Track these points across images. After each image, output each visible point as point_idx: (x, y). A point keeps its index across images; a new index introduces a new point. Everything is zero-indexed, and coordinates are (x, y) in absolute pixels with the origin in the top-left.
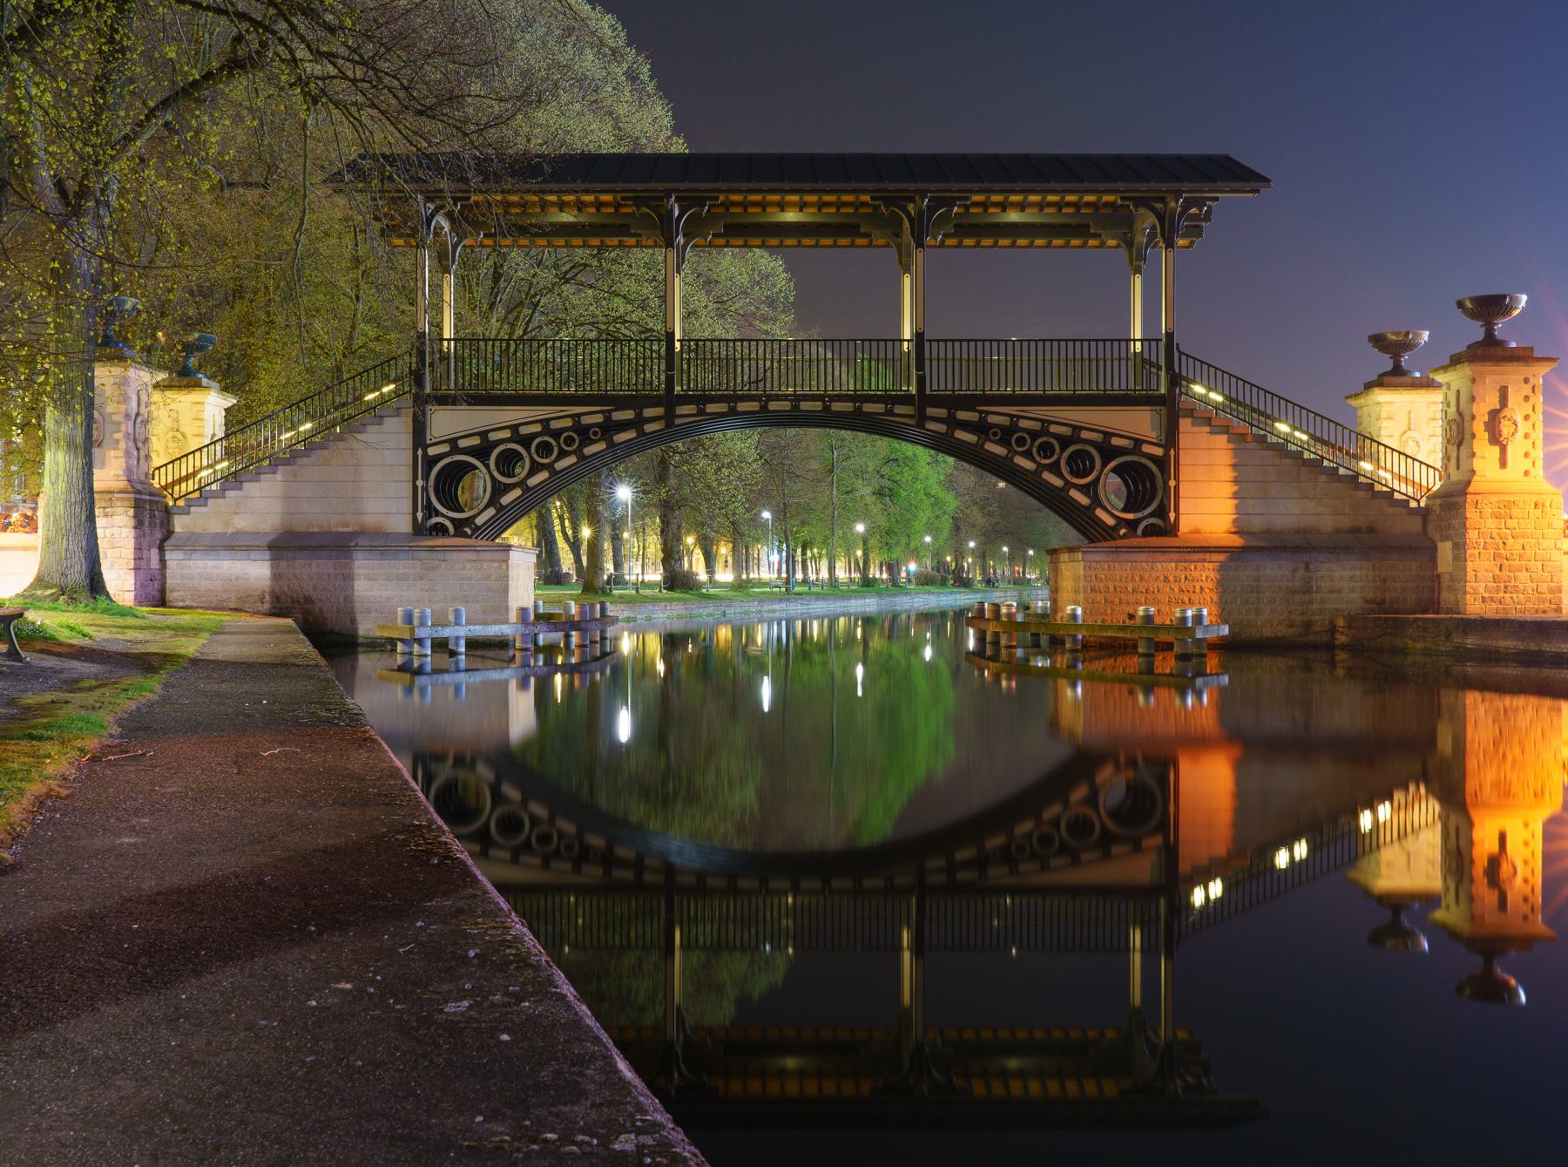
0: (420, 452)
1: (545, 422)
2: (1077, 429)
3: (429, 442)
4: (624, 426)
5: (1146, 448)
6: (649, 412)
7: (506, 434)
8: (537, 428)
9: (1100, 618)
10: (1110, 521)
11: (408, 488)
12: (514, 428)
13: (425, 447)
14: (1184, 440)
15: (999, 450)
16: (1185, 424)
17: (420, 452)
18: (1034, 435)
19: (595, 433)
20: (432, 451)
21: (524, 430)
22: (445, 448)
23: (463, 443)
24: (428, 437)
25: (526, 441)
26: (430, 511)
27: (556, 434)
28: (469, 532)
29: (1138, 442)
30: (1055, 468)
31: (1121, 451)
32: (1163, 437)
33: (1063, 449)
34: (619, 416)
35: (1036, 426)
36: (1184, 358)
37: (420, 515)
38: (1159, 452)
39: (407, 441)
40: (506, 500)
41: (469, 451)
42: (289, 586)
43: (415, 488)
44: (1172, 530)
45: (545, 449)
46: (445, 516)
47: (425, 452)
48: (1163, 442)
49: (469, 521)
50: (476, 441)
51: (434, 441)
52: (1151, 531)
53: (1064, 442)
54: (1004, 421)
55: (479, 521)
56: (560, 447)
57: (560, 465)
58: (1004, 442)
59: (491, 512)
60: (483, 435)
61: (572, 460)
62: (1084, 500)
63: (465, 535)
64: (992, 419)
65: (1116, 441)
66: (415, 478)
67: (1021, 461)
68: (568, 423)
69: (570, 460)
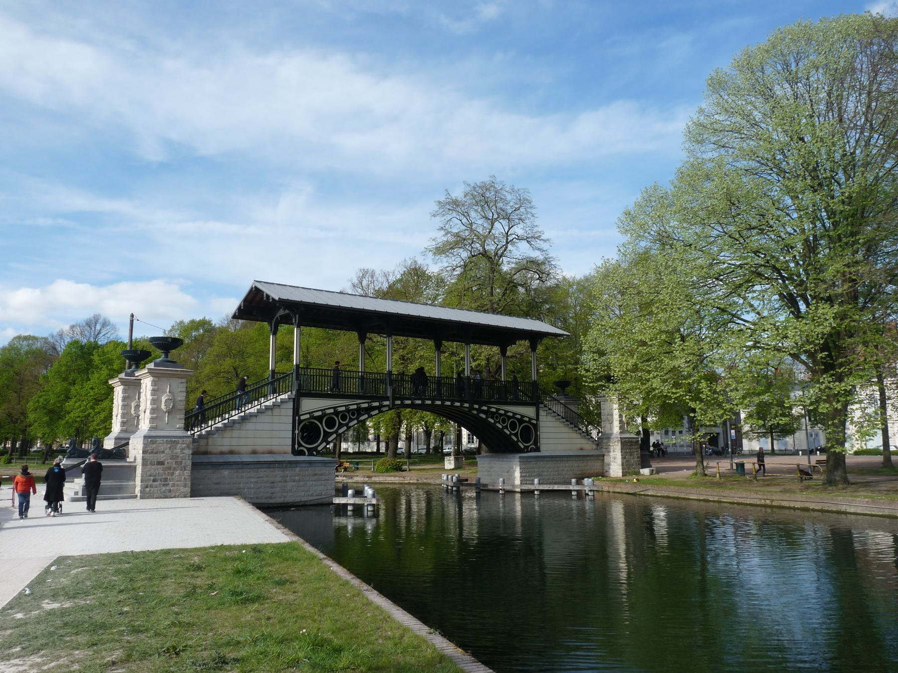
0: (297, 418)
2: (515, 414)
3: (300, 413)
8: (343, 409)
10: (522, 447)
12: (334, 408)
14: (541, 418)
15: (492, 421)
17: (297, 418)
20: (302, 418)
22: (308, 416)
23: (316, 414)
24: (300, 411)
25: (336, 413)
26: (300, 445)
29: (530, 419)
31: (526, 422)
37: (296, 446)
38: (534, 422)
39: (291, 412)
49: (315, 449)
50: (320, 413)
51: (302, 413)
52: (532, 450)
53: (509, 417)
55: (320, 448)
56: (350, 417)
58: (492, 418)
61: (355, 422)
63: (314, 455)
68: (355, 407)
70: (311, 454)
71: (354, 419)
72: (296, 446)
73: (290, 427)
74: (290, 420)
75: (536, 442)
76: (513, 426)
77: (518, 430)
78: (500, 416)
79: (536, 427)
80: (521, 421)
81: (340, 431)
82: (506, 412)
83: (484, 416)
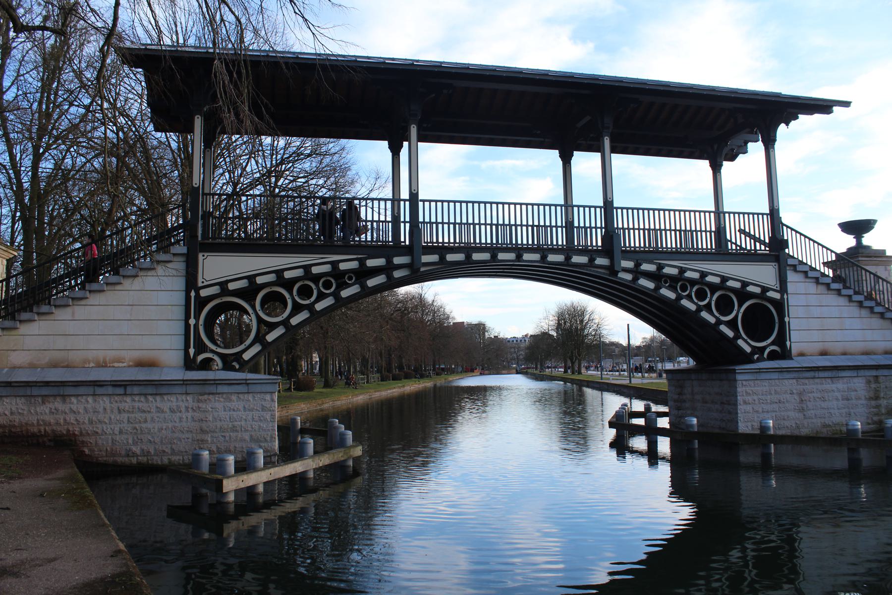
0: (193, 294)
1: (307, 268)
2: (724, 279)
3: (200, 284)
4: (376, 271)
5: (770, 294)
6: (397, 260)
7: (271, 278)
8: (299, 273)
9: (749, 424)
10: (748, 349)
11: (179, 328)
12: (279, 273)
13: (197, 290)
14: (790, 288)
15: (671, 295)
16: (791, 276)
17: (193, 294)
18: (693, 282)
19: (350, 278)
20: (204, 293)
21: (288, 275)
22: (215, 290)
23: (232, 286)
24: (200, 280)
25: (289, 285)
26: (201, 347)
27: (316, 278)
28: (237, 367)
29: (765, 289)
30: (708, 308)
31: (752, 295)
32: (778, 285)
33: (712, 294)
34: (371, 263)
35: (696, 275)
36: (785, 228)
37: (192, 351)
38: (777, 296)
40: (270, 337)
41: (237, 293)
42: (65, 420)
43: (187, 326)
44: (784, 353)
45: (305, 292)
46: (215, 351)
47: (197, 293)
48: (778, 289)
49: (238, 356)
50: (243, 284)
51: (206, 283)
52: (773, 356)
53: (714, 288)
54: (674, 271)
55: (247, 356)
56: (319, 290)
57: (319, 307)
58: (672, 288)
59: (257, 348)
60: (251, 278)
62: (730, 334)
63: (233, 369)
64: (667, 270)
65: (751, 289)
66: (187, 317)
67: (685, 303)
68: (327, 268)
69: (328, 302)
70: (227, 367)
71: (327, 296)
72: (192, 351)
73: (179, 313)
74: (180, 298)
75: (781, 340)
76: (725, 306)
77: (739, 312)
78: (692, 286)
79: (780, 306)
80: (743, 294)
81: (294, 321)
82: (703, 274)
83: (650, 285)
